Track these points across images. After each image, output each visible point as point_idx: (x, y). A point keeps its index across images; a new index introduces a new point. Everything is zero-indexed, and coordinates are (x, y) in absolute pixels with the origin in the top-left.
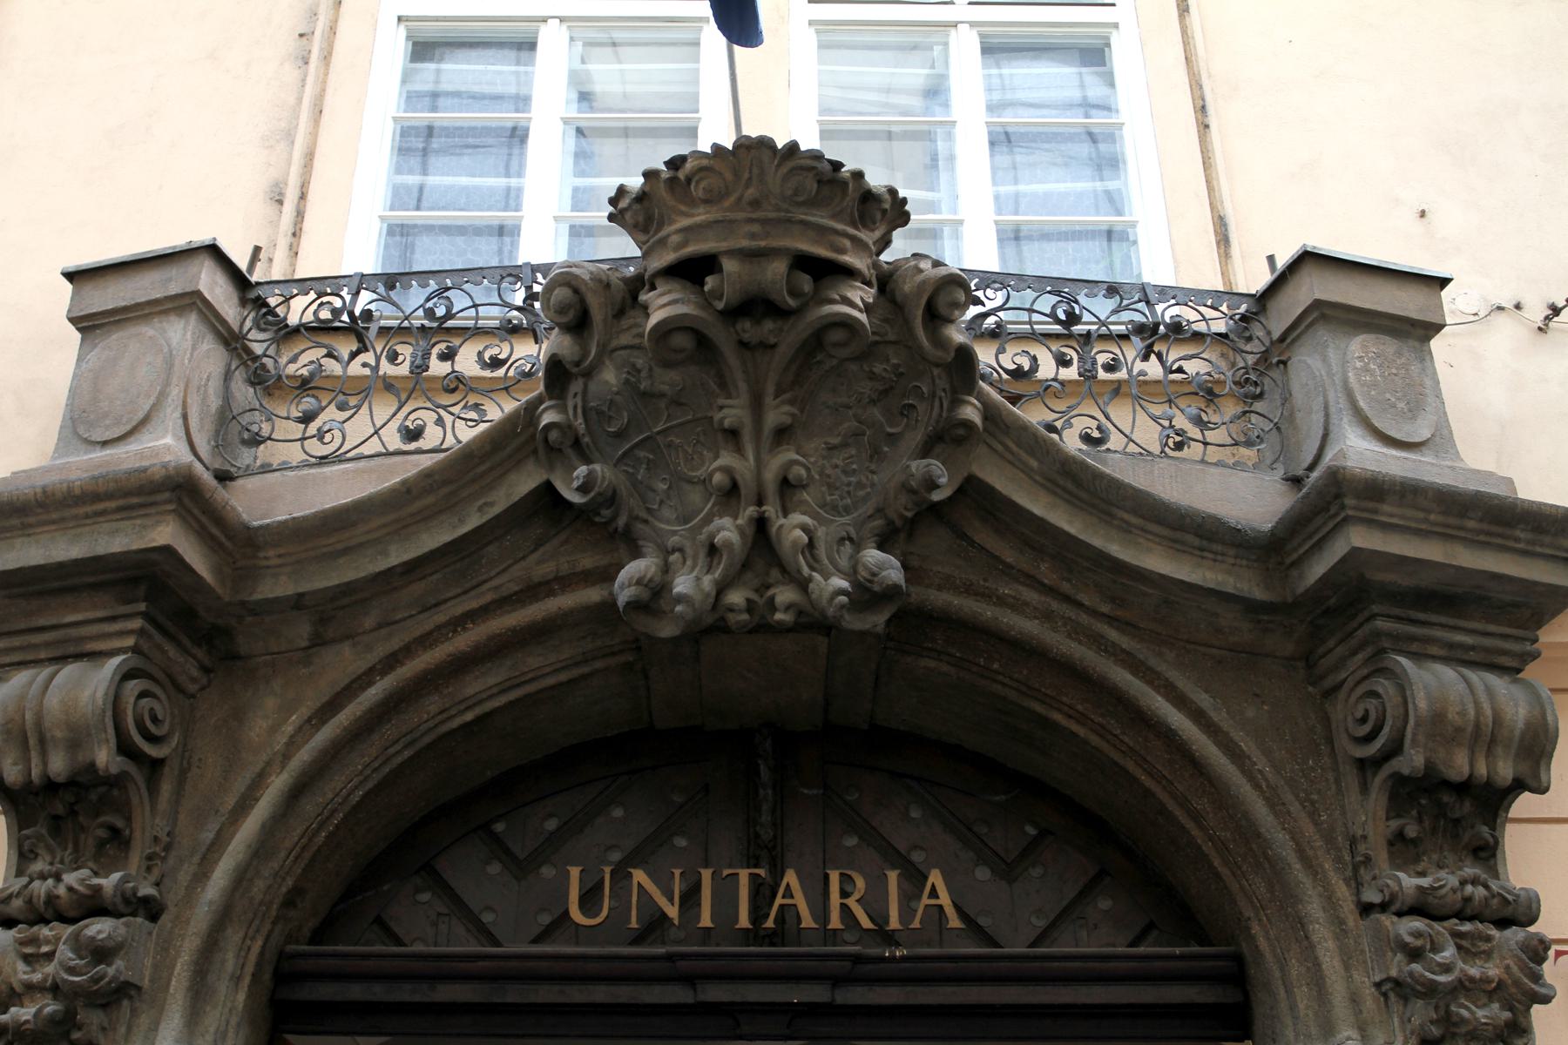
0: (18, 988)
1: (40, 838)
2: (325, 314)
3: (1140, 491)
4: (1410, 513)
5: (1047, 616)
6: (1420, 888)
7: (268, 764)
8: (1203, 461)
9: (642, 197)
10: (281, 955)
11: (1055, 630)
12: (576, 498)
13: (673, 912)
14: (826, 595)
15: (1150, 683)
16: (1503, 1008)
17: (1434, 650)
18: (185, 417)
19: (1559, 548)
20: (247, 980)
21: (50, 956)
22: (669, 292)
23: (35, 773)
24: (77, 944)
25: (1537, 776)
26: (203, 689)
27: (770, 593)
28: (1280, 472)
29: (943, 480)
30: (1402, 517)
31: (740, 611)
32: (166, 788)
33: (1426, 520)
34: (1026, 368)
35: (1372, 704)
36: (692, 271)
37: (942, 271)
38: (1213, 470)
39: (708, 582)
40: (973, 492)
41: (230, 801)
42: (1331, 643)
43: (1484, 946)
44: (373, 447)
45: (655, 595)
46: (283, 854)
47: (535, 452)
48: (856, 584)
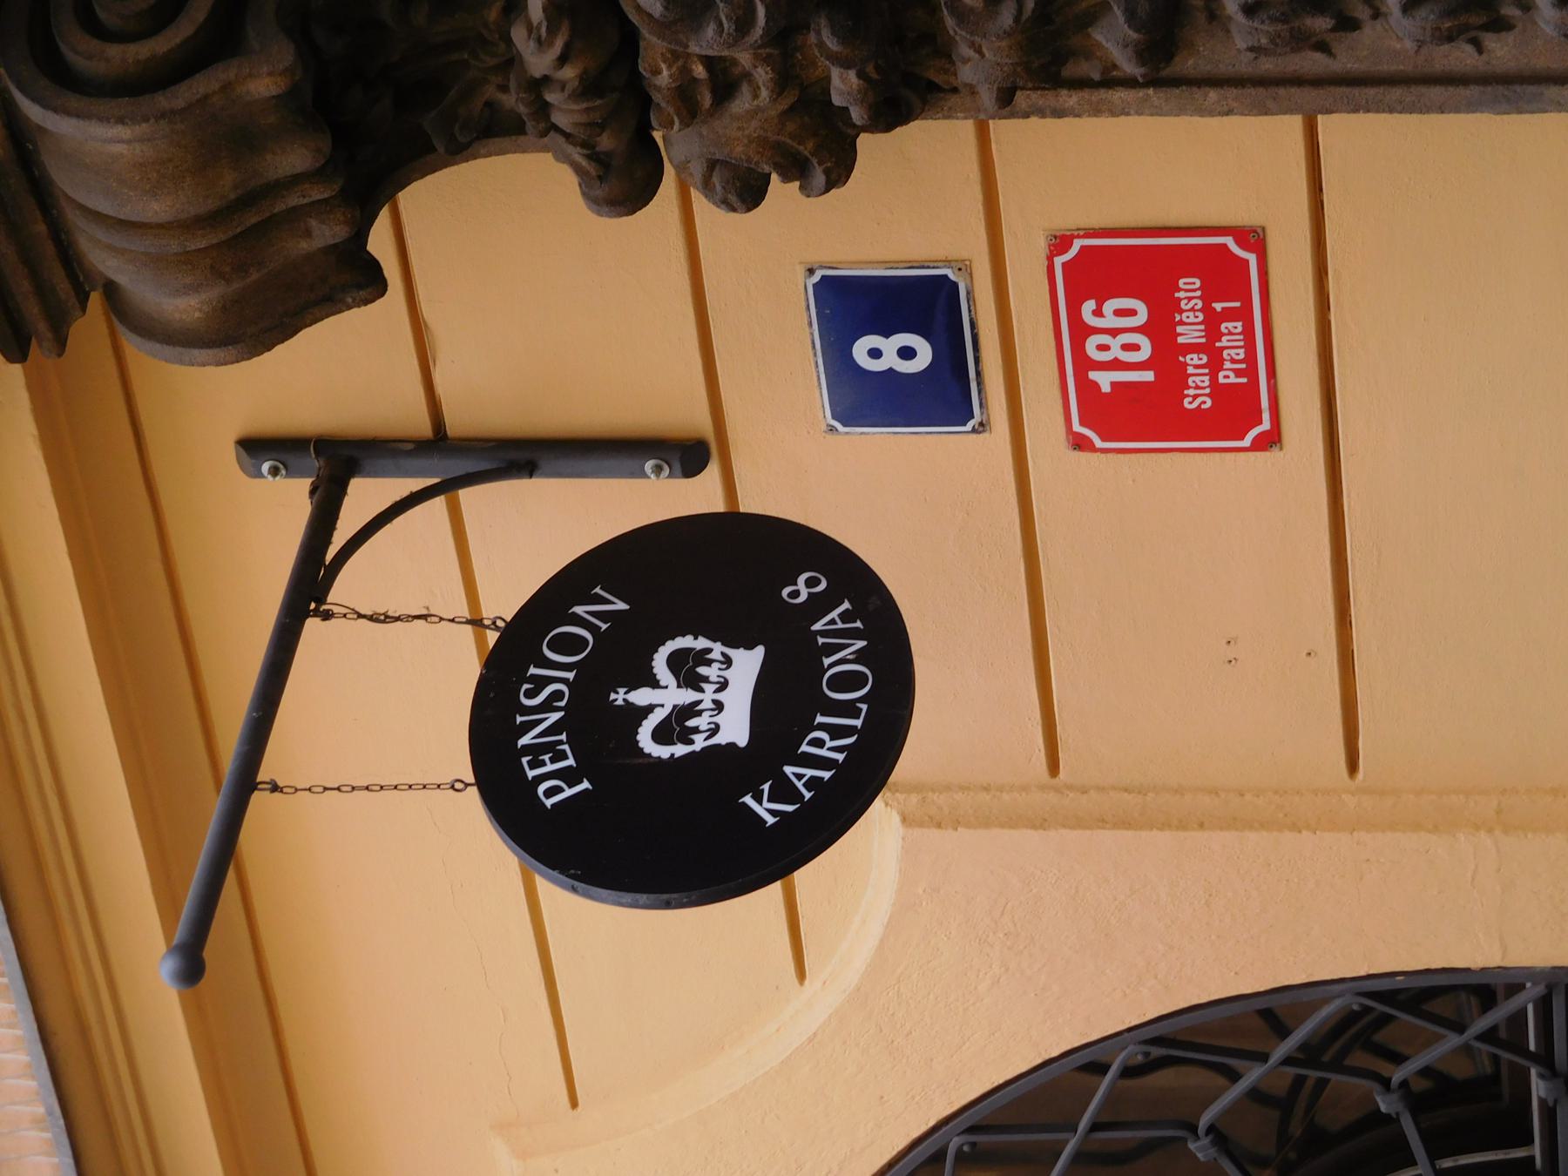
23: (318, 193)
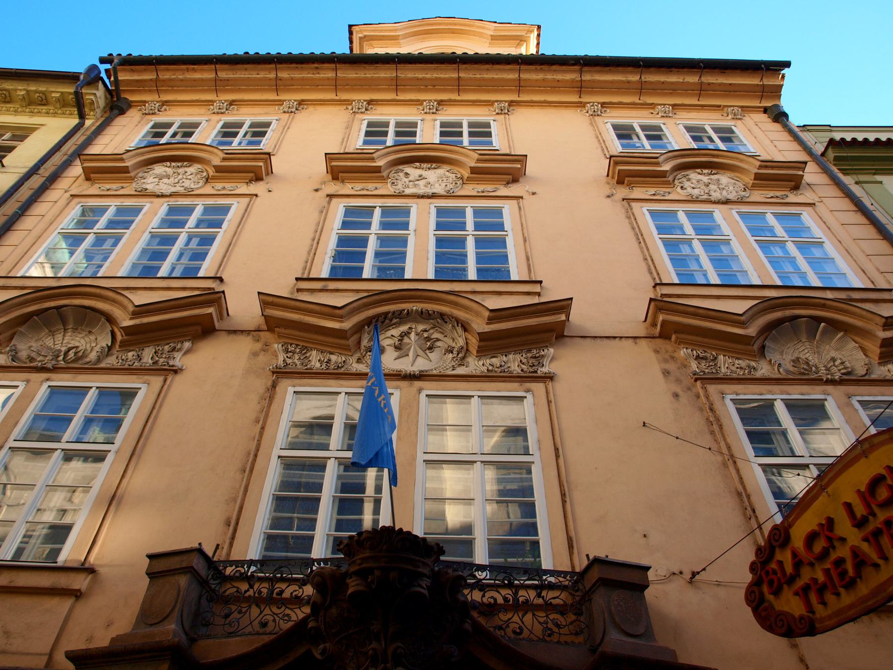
8: (558, 642)
9: (347, 545)
12: (319, 657)
36: (362, 574)
44: (249, 629)
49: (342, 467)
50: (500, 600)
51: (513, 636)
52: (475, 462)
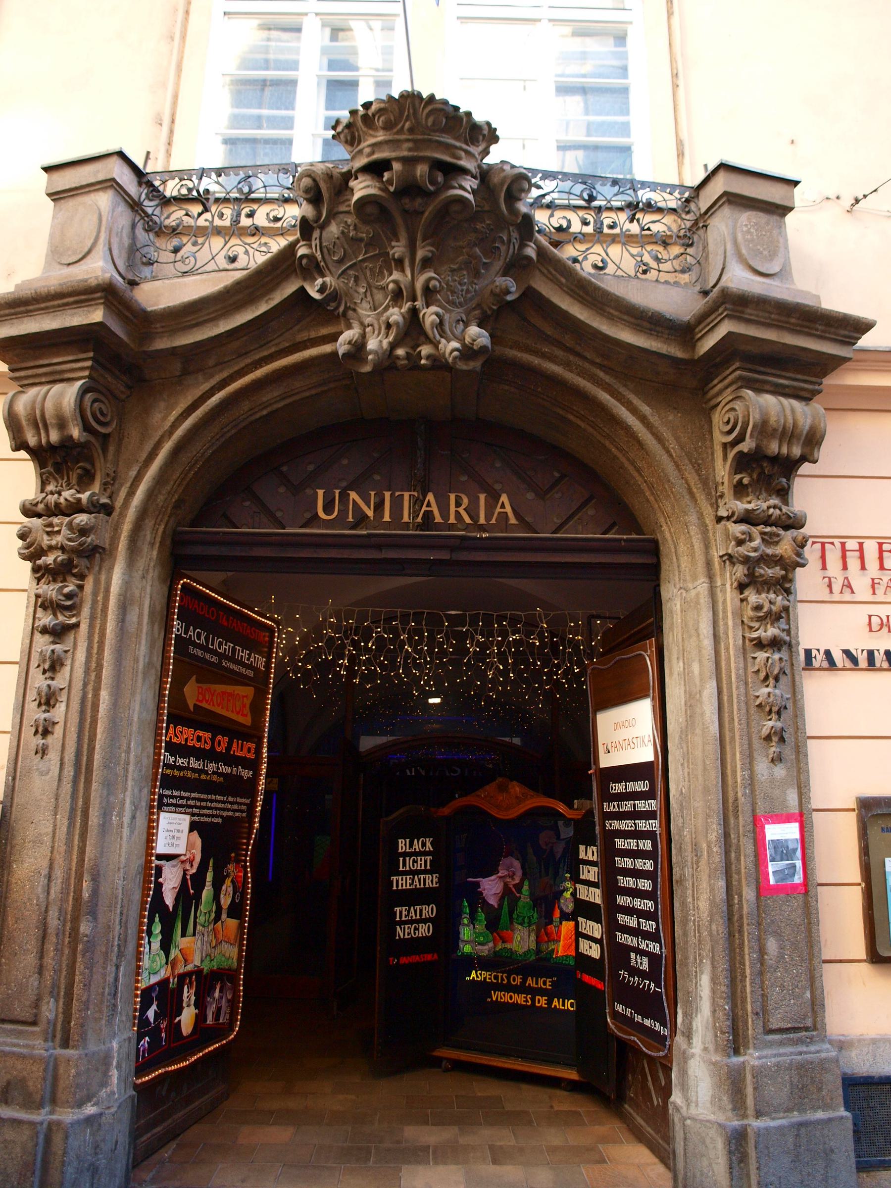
0: (45, 548)
1: (50, 473)
2: (184, 191)
3: (618, 297)
4: (761, 314)
5: (567, 365)
6: (747, 511)
7: (162, 436)
9: (349, 126)
10: (175, 533)
11: (571, 371)
12: (317, 296)
13: (370, 513)
14: (448, 351)
15: (619, 400)
16: (782, 569)
17: (767, 387)
18: (110, 250)
19: (838, 335)
20: (157, 545)
21: (59, 532)
22: (365, 181)
23: (44, 441)
24: (70, 526)
25: (812, 454)
26: (128, 397)
27: (419, 349)
28: (698, 288)
29: (513, 289)
30: (757, 316)
31: (403, 359)
32: (112, 449)
33: (770, 318)
34: (565, 226)
35: (731, 415)
36: (376, 169)
37: (516, 171)
38: (661, 287)
39: (385, 344)
40: (530, 296)
41: (144, 455)
42: (715, 382)
43: (776, 539)
44: (211, 266)
45: (358, 348)
46: (172, 483)
47: (295, 270)
48: (464, 345)
49: (328, 31)
50: (576, 227)
51: (593, 271)
52: (540, 20)
